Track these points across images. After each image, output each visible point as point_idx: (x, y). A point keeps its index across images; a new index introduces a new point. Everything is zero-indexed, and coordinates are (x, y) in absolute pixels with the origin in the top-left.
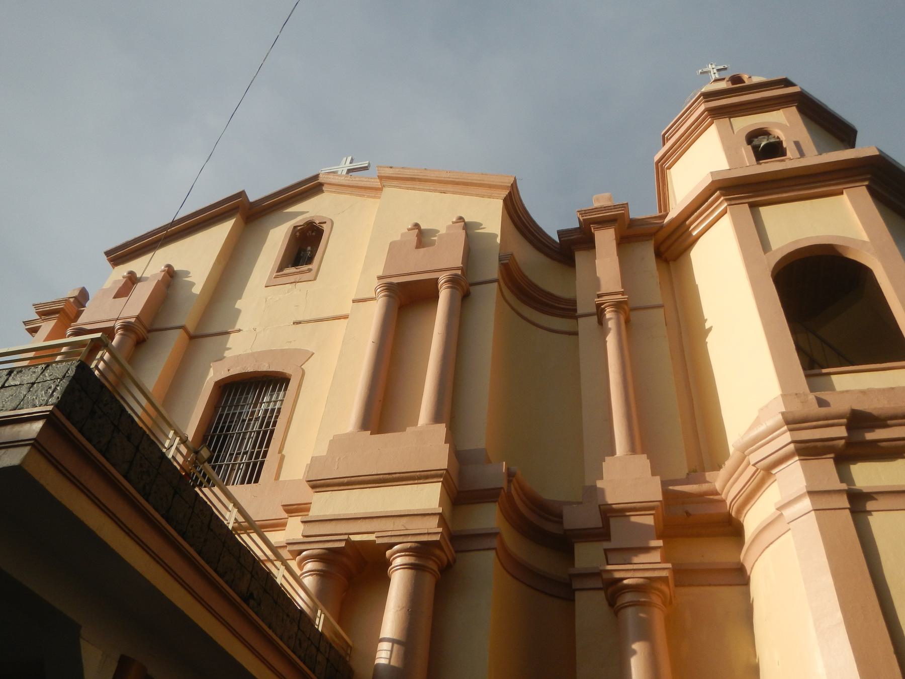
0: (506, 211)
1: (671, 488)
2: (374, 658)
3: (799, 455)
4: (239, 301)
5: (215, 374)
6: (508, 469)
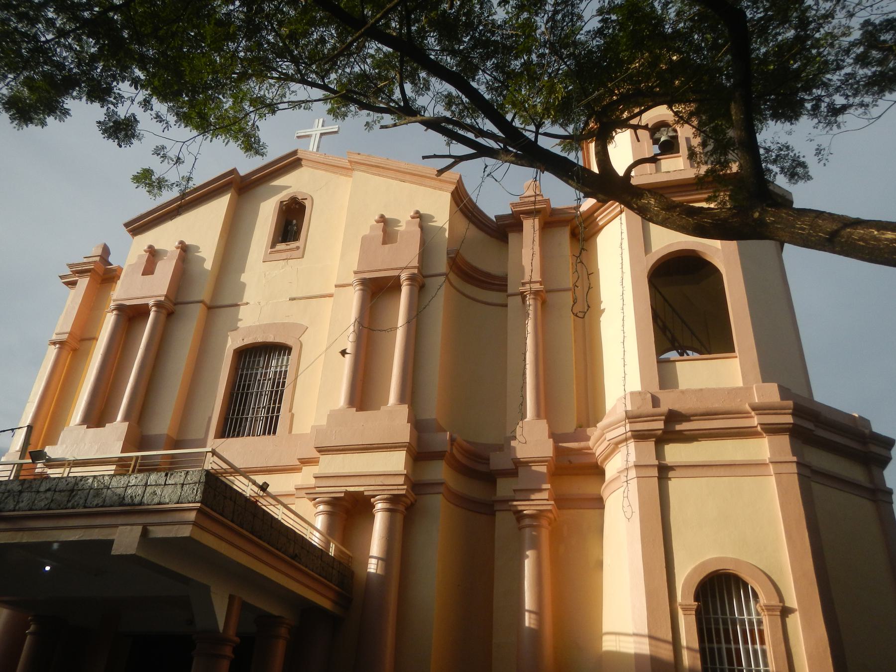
0: (453, 202)
1: (560, 444)
2: (367, 568)
3: (634, 439)
4: (243, 275)
5: (233, 342)
6: (451, 436)
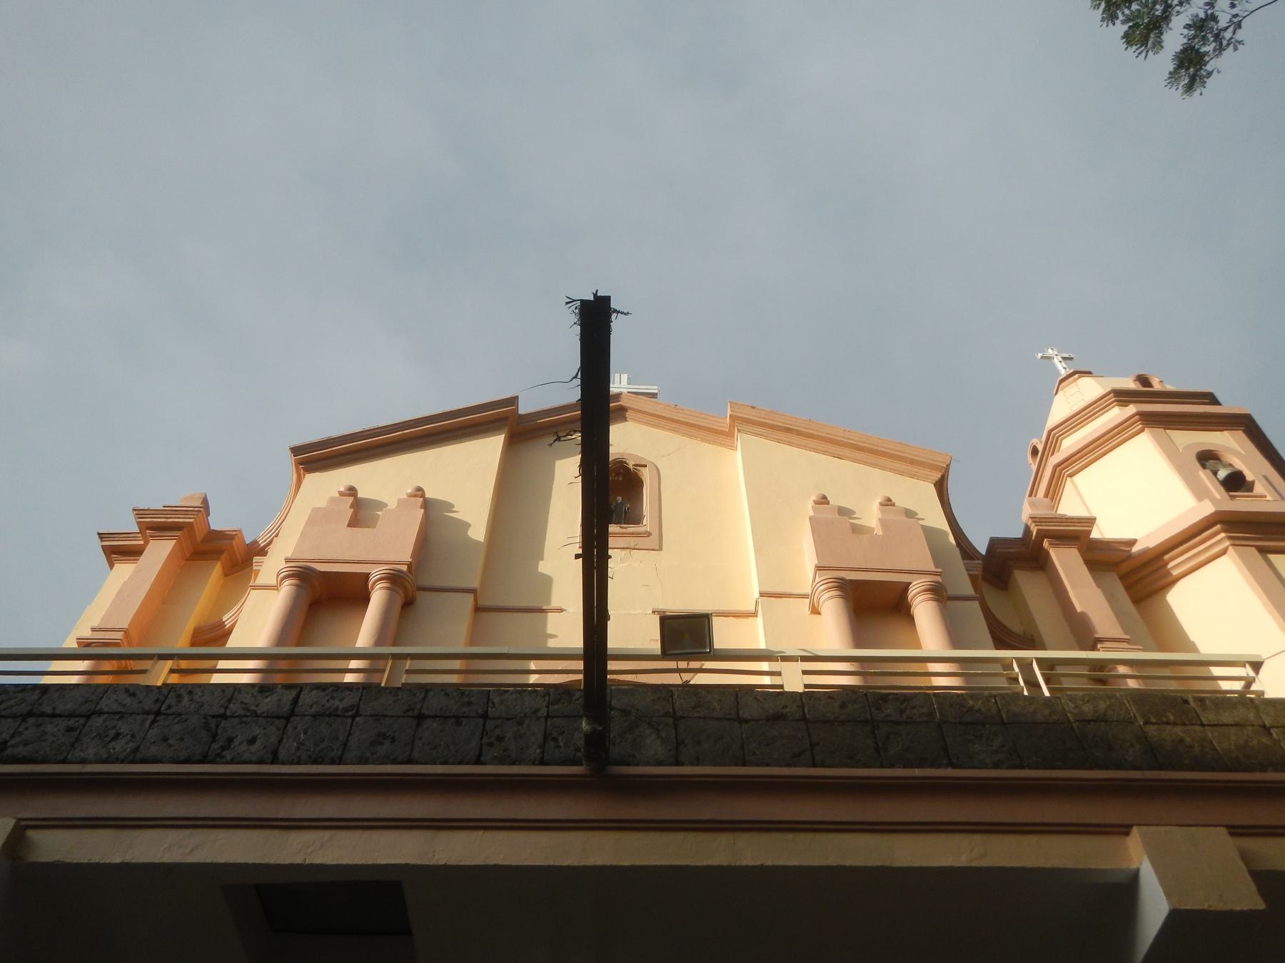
4: (541, 562)
